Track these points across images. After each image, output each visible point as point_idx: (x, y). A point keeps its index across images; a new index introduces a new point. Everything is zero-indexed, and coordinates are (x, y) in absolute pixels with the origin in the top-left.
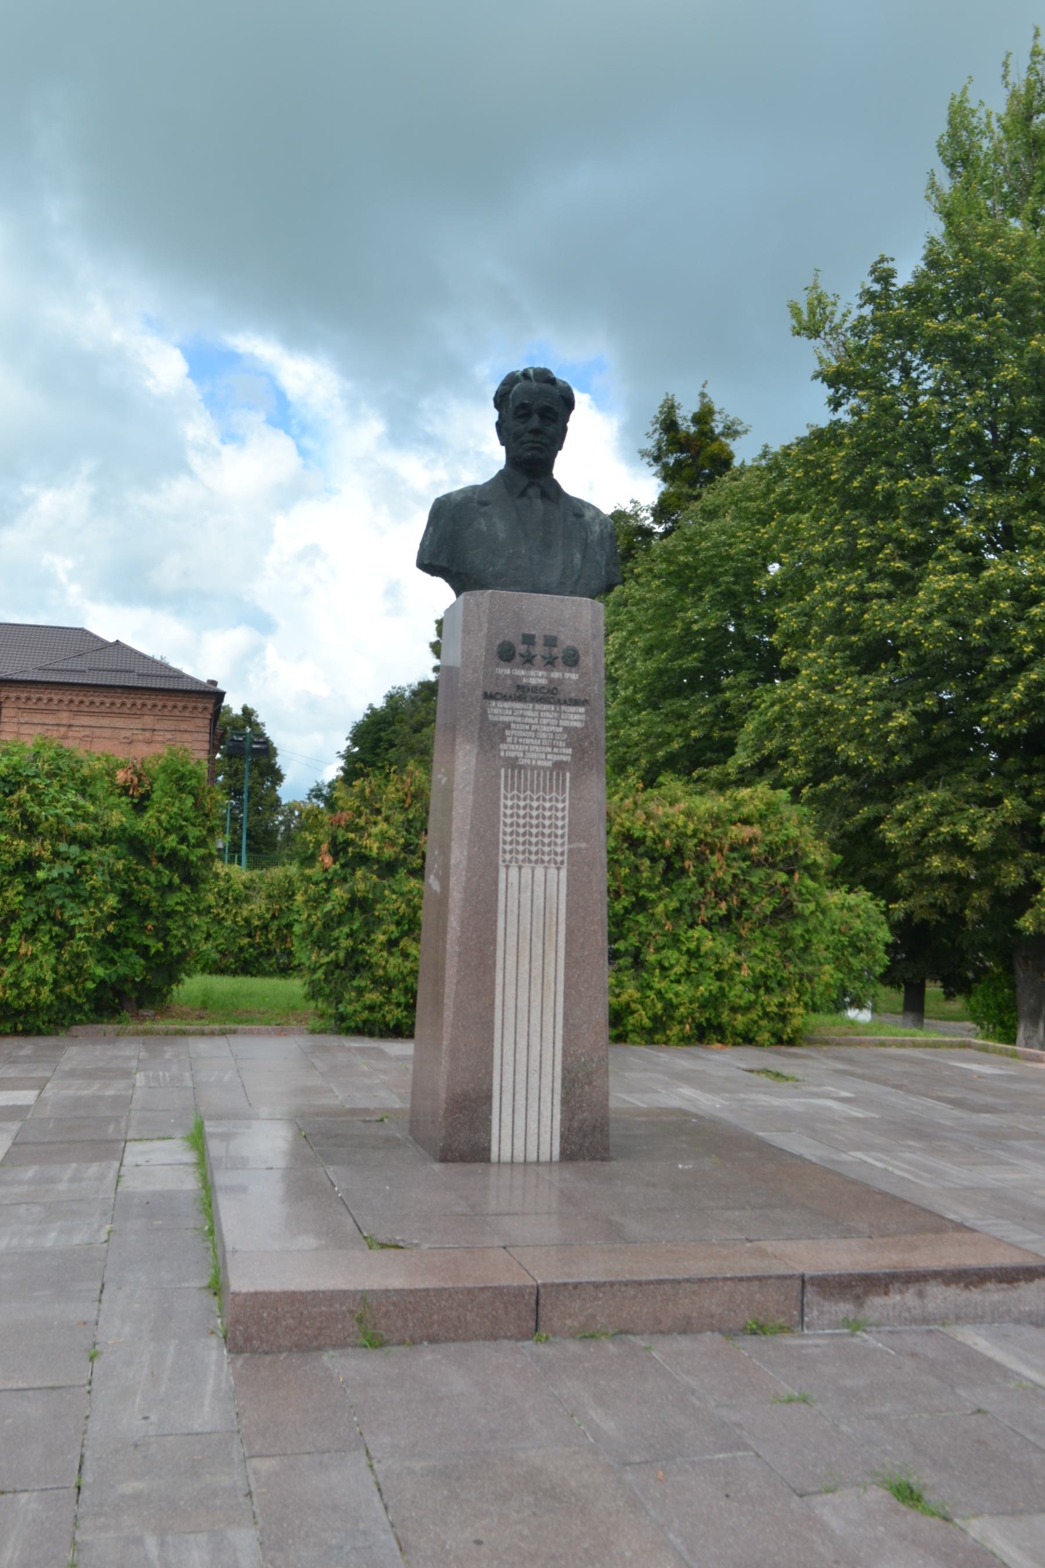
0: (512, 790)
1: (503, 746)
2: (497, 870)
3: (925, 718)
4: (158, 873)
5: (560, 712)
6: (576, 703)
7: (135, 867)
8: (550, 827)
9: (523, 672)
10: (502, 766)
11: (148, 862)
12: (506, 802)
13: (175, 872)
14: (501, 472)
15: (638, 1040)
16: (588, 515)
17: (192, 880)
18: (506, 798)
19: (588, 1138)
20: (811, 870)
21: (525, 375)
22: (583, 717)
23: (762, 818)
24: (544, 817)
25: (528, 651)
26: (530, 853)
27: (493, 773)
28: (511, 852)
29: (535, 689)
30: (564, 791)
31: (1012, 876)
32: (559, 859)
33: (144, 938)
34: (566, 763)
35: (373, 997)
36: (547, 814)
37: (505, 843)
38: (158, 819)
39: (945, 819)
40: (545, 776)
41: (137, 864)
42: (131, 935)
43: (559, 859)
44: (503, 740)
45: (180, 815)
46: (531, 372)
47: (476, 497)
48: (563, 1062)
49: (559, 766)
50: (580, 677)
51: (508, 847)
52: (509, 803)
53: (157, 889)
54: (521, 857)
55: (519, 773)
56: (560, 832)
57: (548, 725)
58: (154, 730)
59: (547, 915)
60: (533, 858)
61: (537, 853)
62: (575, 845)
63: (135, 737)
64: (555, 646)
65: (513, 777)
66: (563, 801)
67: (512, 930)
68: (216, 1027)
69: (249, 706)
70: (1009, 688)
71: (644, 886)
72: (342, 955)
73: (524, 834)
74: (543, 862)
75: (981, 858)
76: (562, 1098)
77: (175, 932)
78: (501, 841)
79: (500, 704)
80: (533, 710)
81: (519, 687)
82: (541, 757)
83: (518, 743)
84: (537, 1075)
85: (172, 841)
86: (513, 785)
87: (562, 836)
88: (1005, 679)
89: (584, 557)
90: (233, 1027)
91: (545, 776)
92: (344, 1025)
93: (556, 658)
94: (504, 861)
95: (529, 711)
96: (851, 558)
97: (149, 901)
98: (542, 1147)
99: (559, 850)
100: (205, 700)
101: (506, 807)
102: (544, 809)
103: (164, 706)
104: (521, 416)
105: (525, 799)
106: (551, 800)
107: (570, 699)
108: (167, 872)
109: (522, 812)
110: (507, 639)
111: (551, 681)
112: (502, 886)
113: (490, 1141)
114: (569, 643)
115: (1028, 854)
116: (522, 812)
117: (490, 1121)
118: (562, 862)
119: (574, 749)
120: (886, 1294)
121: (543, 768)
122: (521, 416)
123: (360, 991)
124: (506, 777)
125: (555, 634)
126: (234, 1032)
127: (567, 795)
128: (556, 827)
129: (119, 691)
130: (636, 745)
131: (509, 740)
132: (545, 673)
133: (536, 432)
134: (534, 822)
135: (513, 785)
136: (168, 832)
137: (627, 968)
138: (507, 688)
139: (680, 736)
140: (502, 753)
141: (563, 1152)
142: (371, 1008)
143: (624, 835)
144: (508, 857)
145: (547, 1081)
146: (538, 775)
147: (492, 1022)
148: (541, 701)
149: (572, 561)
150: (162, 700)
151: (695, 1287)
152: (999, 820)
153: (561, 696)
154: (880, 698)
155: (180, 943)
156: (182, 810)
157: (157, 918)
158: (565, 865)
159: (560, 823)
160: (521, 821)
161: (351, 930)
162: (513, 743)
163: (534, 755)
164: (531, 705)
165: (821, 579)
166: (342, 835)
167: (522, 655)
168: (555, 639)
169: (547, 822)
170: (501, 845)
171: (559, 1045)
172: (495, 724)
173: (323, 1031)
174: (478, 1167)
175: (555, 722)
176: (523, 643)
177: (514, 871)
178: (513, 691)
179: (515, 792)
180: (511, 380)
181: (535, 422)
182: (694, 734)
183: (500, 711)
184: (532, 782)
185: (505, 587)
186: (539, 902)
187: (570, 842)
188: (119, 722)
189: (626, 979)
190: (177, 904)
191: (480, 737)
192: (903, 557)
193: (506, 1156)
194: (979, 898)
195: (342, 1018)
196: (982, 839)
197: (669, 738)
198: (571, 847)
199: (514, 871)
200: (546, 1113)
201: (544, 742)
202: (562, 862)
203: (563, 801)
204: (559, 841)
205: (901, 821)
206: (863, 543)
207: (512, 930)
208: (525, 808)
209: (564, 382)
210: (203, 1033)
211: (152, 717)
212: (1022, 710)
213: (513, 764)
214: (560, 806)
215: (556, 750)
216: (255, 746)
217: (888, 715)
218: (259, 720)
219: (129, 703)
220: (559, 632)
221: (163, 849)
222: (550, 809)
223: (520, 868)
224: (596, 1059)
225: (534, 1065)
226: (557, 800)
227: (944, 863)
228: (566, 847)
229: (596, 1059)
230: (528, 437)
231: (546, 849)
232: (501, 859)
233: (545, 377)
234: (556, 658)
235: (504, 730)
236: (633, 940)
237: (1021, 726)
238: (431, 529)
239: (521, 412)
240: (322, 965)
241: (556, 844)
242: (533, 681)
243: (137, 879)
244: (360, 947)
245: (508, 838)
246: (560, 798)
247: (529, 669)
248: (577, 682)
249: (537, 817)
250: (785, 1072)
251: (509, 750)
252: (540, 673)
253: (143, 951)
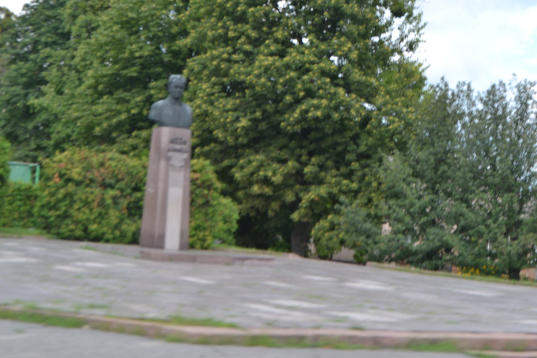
3: (255, 121)
20: (216, 189)
23: (200, 171)
31: (290, 197)
35: (72, 227)
39: (262, 169)
49: (182, 167)
70: (294, 111)
75: (276, 188)
88: (292, 106)
96: (225, 40)
115: (297, 187)
123: (67, 225)
130: (100, 115)
139: (125, 112)
142: (71, 231)
152: (286, 171)
154: (235, 110)
165: (210, 48)
166: (63, 172)
182: (133, 111)
183: (171, 154)
192: (250, 43)
194: (275, 205)
196: (277, 179)
197: (119, 113)
205: (242, 168)
206: (231, 34)
212: (298, 122)
213: (173, 166)
217: (237, 119)
227: (259, 188)
237: (298, 128)
251: (172, 162)
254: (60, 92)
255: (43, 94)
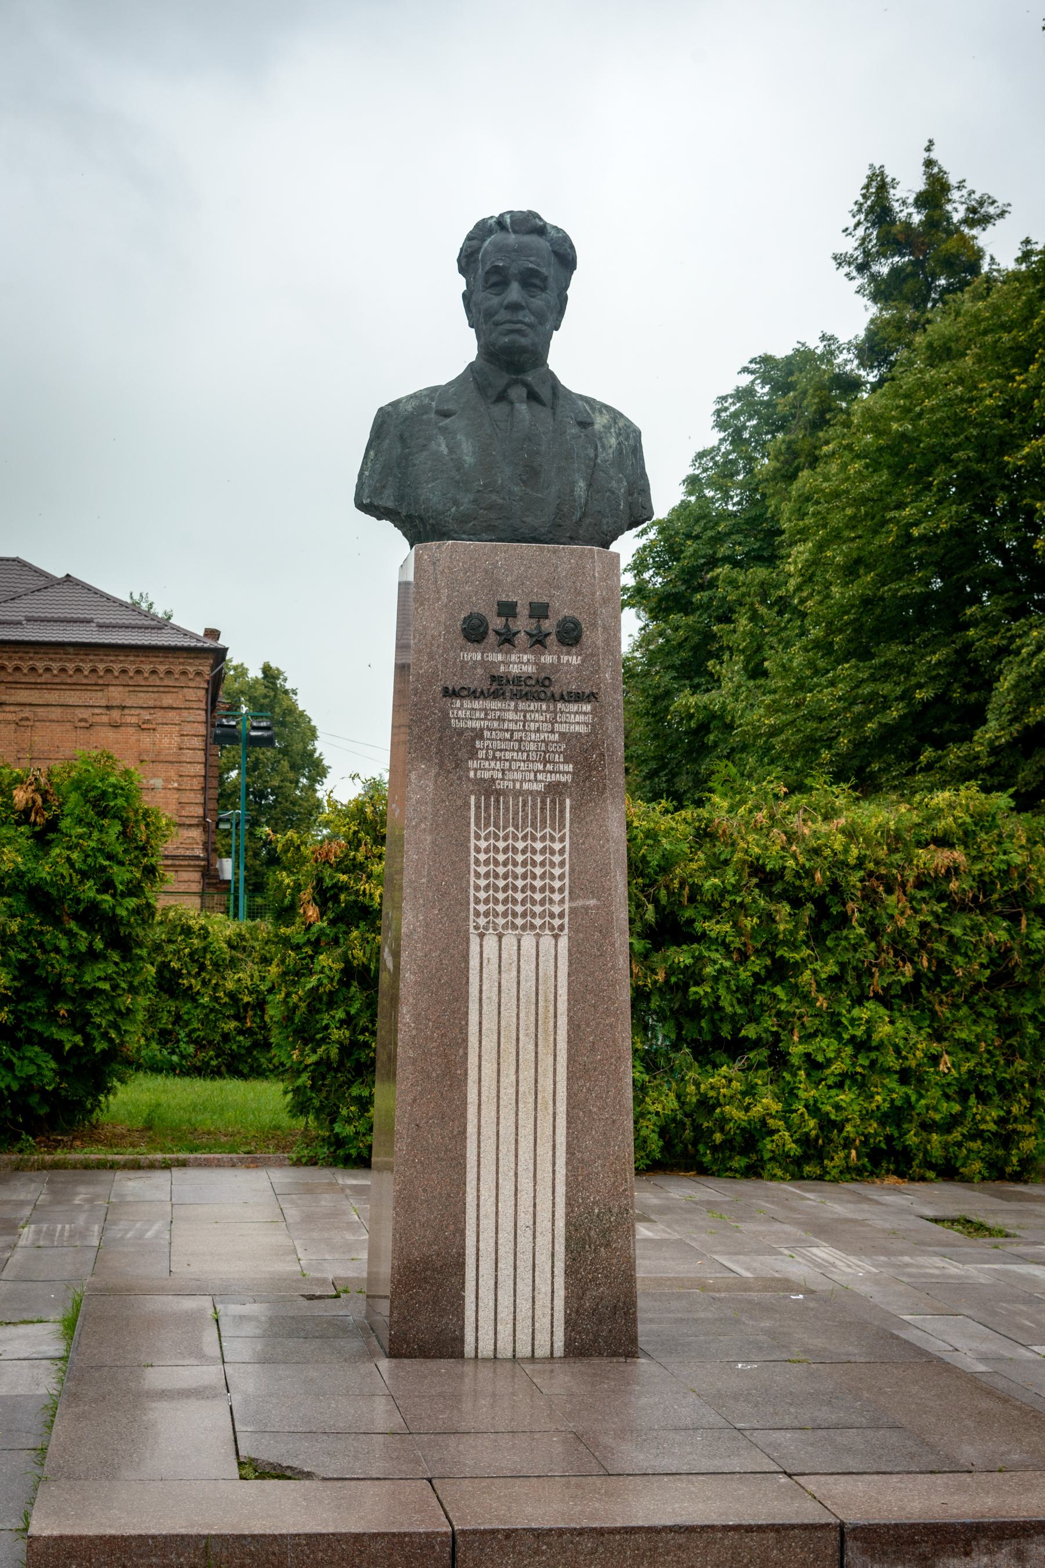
0: (487, 825)
1: (473, 764)
2: (467, 941)
4: (70, 934)
5: (555, 712)
6: (578, 697)
7: (39, 928)
8: (543, 877)
9: (500, 657)
10: (472, 792)
11: (57, 922)
12: (478, 843)
13: (97, 932)
14: (471, 365)
15: (780, 1173)
16: (600, 421)
17: (123, 944)
18: (478, 837)
19: (603, 1326)
21: (500, 222)
22: (589, 719)
23: (967, 838)
24: (534, 863)
25: (506, 626)
26: (515, 915)
27: (459, 802)
28: (486, 914)
29: (518, 680)
30: (562, 826)
32: (557, 922)
33: (54, 1030)
34: (565, 784)
36: (538, 858)
37: (477, 901)
38: (68, 859)
40: (534, 805)
41: (41, 924)
42: (38, 1027)
43: (557, 922)
44: (473, 754)
45: (99, 850)
46: (508, 219)
47: (434, 404)
48: (567, 1214)
49: (554, 790)
50: (583, 661)
51: (482, 908)
52: (483, 844)
53: (71, 959)
54: (501, 921)
55: (497, 801)
56: (557, 884)
57: (538, 731)
58: (124, 708)
59: (541, 1003)
60: (519, 922)
61: (524, 915)
62: (580, 903)
63: (96, 719)
64: (547, 617)
65: (487, 807)
66: (562, 839)
67: (490, 1025)
68: (159, 1156)
69: (273, 665)
71: (785, 943)
72: (334, 1052)
73: (505, 889)
74: (533, 927)
76: (567, 1267)
77: (98, 1020)
78: (472, 899)
79: (467, 704)
80: (516, 710)
81: (493, 678)
82: (527, 778)
83: (494, 758)
84: (530, 1232)
85: (89, 890)
86: (488, 818)
87: (561, 890)
89: (590, 485)
90: (182, 1156)
91: (534, 805)
92: (341, 1152)
93: (549, 634)
94: (476, 928)
95: (509, 711)
97: (60, 975)
98: (538, 1336)
99: (556, 909)
100: (197, 662)
101: (478, 850)
102: (534, 851)
103: (138, 672)
104: (494, 285)
105: (505, 839)
106: (543, 839)
107: (569, 693)
108: (85, 934)
109: (501, 858)
110: (476, 610)
111: (541, 667)
112: (474, 963)
113: (462, 1328)
114: (566, 612)
116: (501, 858)
117: (463, 1298)
118: (561, 928)
119: (575, 764)
120: (967, 1554)
121: (531, 792)
122: (494, 285)
124: (478, 807)
125: (546, 600)
126: (183, 1164)
127: (567, 830)
128: (552, 877)
129: (71, 650)
130: (832, 716)
131: (481, 754)
132: (532, 657)
133: (514, 307)
134: (520, 870)
135: (488, 818)
136: (84, 875)
137: (761, 1066)
138: (478, 680)
139: (900, 698)
140: (472, 774)
141: (568, 1343)
143: (751, 865)
144: (482, 921)
145: (543, 1241)
146: (525, 804)
147: (464, 1156)
148: (526, 697)
149: (572, 491)
150: (133, 662)
151: (681, 1539)
153: (556, 689)
155: (105, 1035)
156: (103, 843)
157: (73, 1000)
158: (566, 931)
159: (557, 872)
160: (501, 870)
161: (348, 1013)
162: (487, 759)
163: (518, 776)
164: (513, 704)
167: (497, 633)
168: (546, 606)
169: (538, 871)
170: (472, 905)
171: (561, 1189)
172: (461, 732)
173: (312, 1162)
174: (444, 1365)
175: (547, 727)
176: (499, 615)
177: (491, 942)
178: (485, 685)
179: (492, 828)
180: (482, 230)
181: (515, 292)
183: (467, 714)
184: (516, 813)
185: (474, 535)
186: (528, 986)
187: (571, 899)
188: (72, 697)
189: (760, 1082)
190: (99, 979)
191: (439, 752)
193: (486, 1349)
195: (339, 1142)
197: (885, 704)
198: (574, 905)
199: (491, 942)
200: (544, 1288)
201: (533, 756)
202: (561, 928)
203: (562, 839)
204: (556, 897)
207: (490, 1025)
208: (505, 850)
209: (558, 230)
210: (136, 1166)
211: (121, 689)
213: (488, 789)
214: (557, 846)
215: (549, 767)
216: (253, 733)
218: (288, 686)
219: (87, 667)
220: (551, 596)
221: (78, 901)
222: (543, 851)
223: (500, 937)
224: (616, 1210)
225: (525, 1219)
226: (552, 839)
228: (566, 906)
229: (616, 1210)
230: (503, 315)
231: (538, 909)
232: (472, 924)
233: (528, 224)
234: (549, 634)
235: (473, 740)
236: (769, 1022)
238: (372, 453)
239: (494, 279)
240: (307, 1066)
241: (551, 901)
242: (515, 670)
243: (41, 945)
244: (361, 1038)
245: (482, 895)
246: (557, 836)
247: (508, 652)
248: (579, 668)
249: (524, 864)
250: (990, 1222)
252: (525, 658)
253: (53, 1047)
254: (757, 672)
255: (715, 681)
